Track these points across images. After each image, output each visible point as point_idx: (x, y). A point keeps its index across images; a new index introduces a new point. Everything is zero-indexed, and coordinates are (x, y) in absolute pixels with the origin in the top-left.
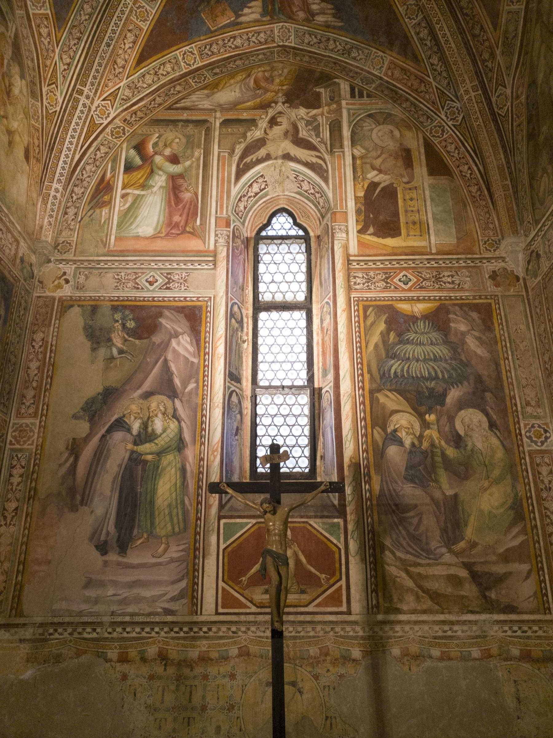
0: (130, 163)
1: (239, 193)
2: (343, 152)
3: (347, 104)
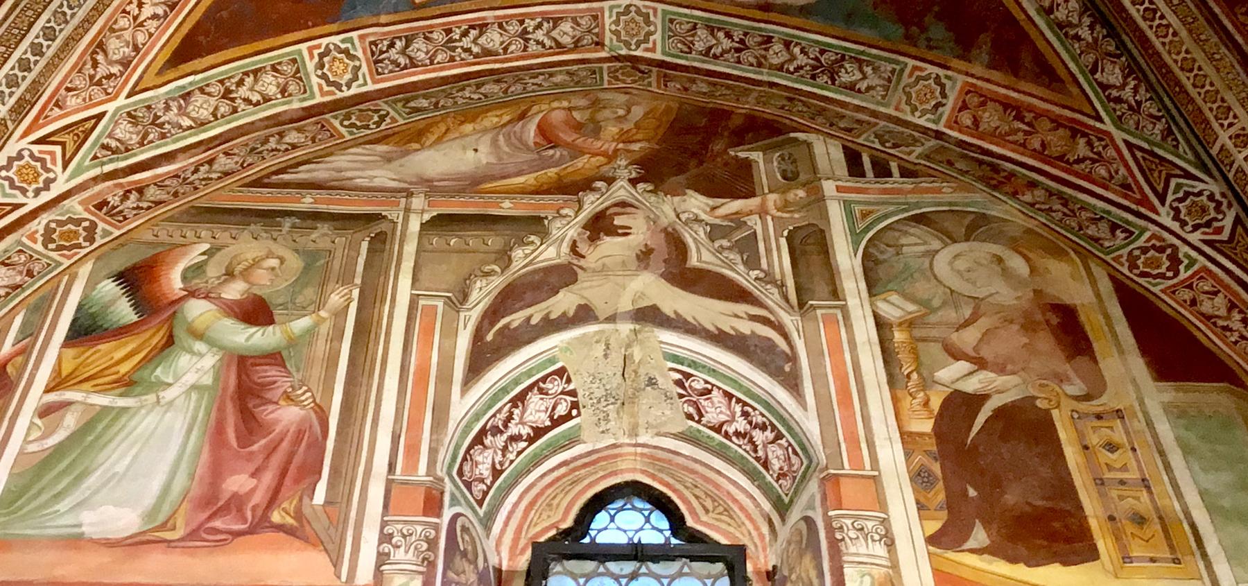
0: (93, 316)
1: (477, 418)
2: (844, 310)
3: (838, 189)
